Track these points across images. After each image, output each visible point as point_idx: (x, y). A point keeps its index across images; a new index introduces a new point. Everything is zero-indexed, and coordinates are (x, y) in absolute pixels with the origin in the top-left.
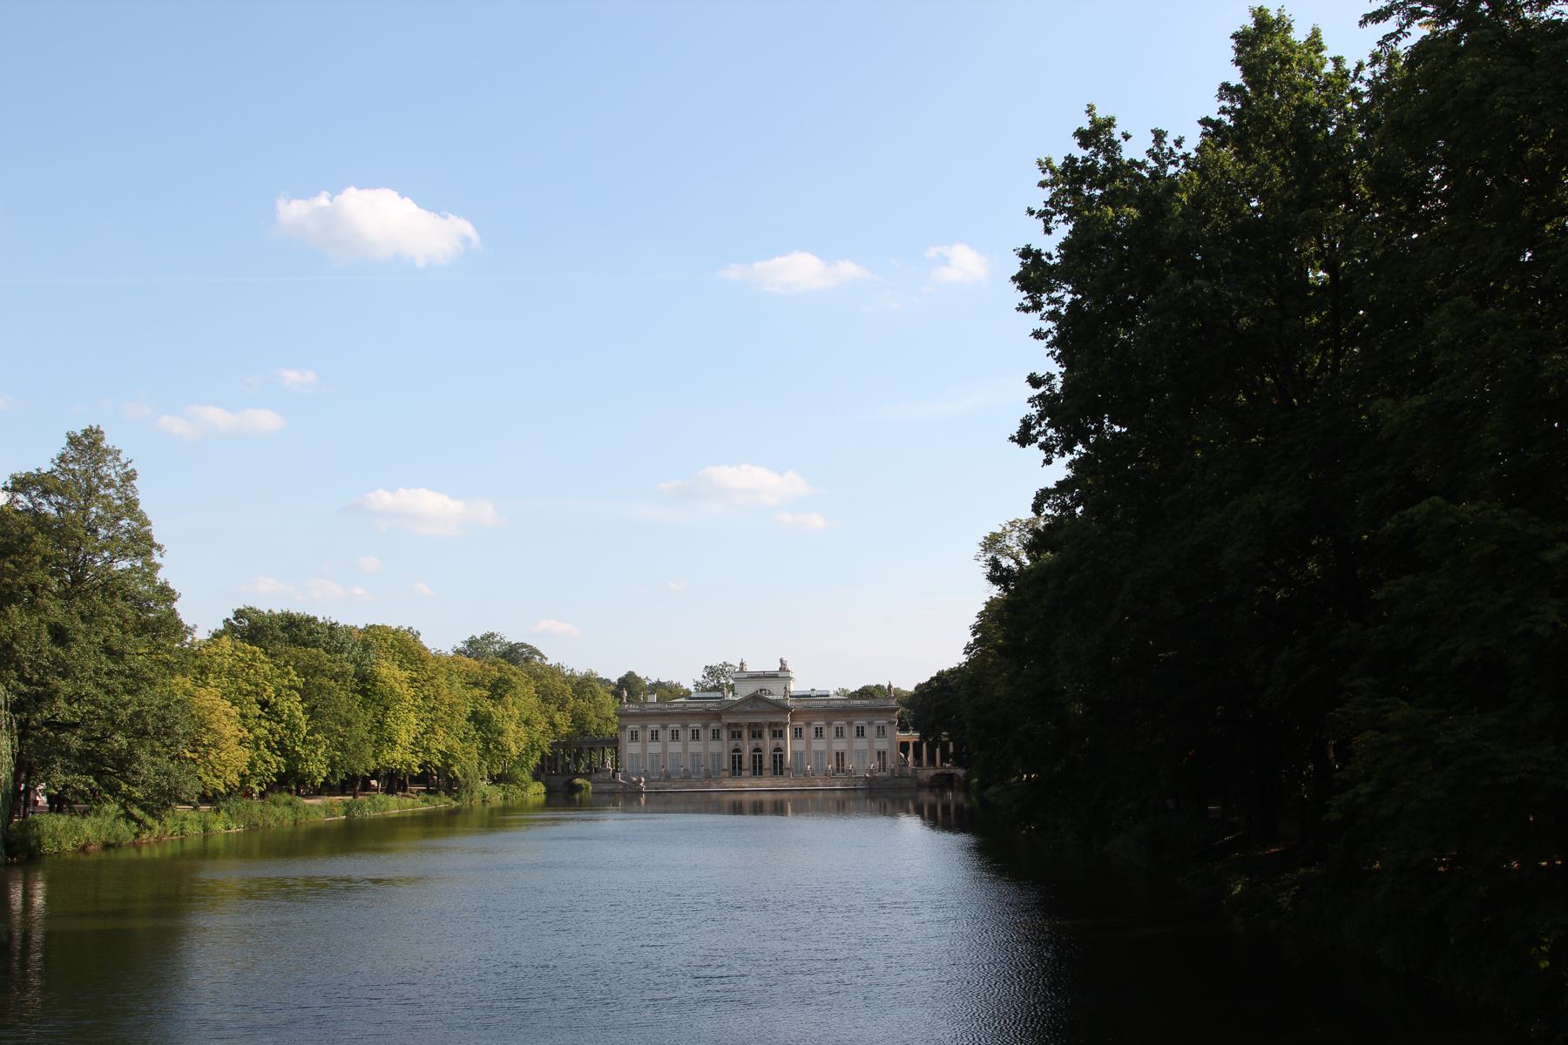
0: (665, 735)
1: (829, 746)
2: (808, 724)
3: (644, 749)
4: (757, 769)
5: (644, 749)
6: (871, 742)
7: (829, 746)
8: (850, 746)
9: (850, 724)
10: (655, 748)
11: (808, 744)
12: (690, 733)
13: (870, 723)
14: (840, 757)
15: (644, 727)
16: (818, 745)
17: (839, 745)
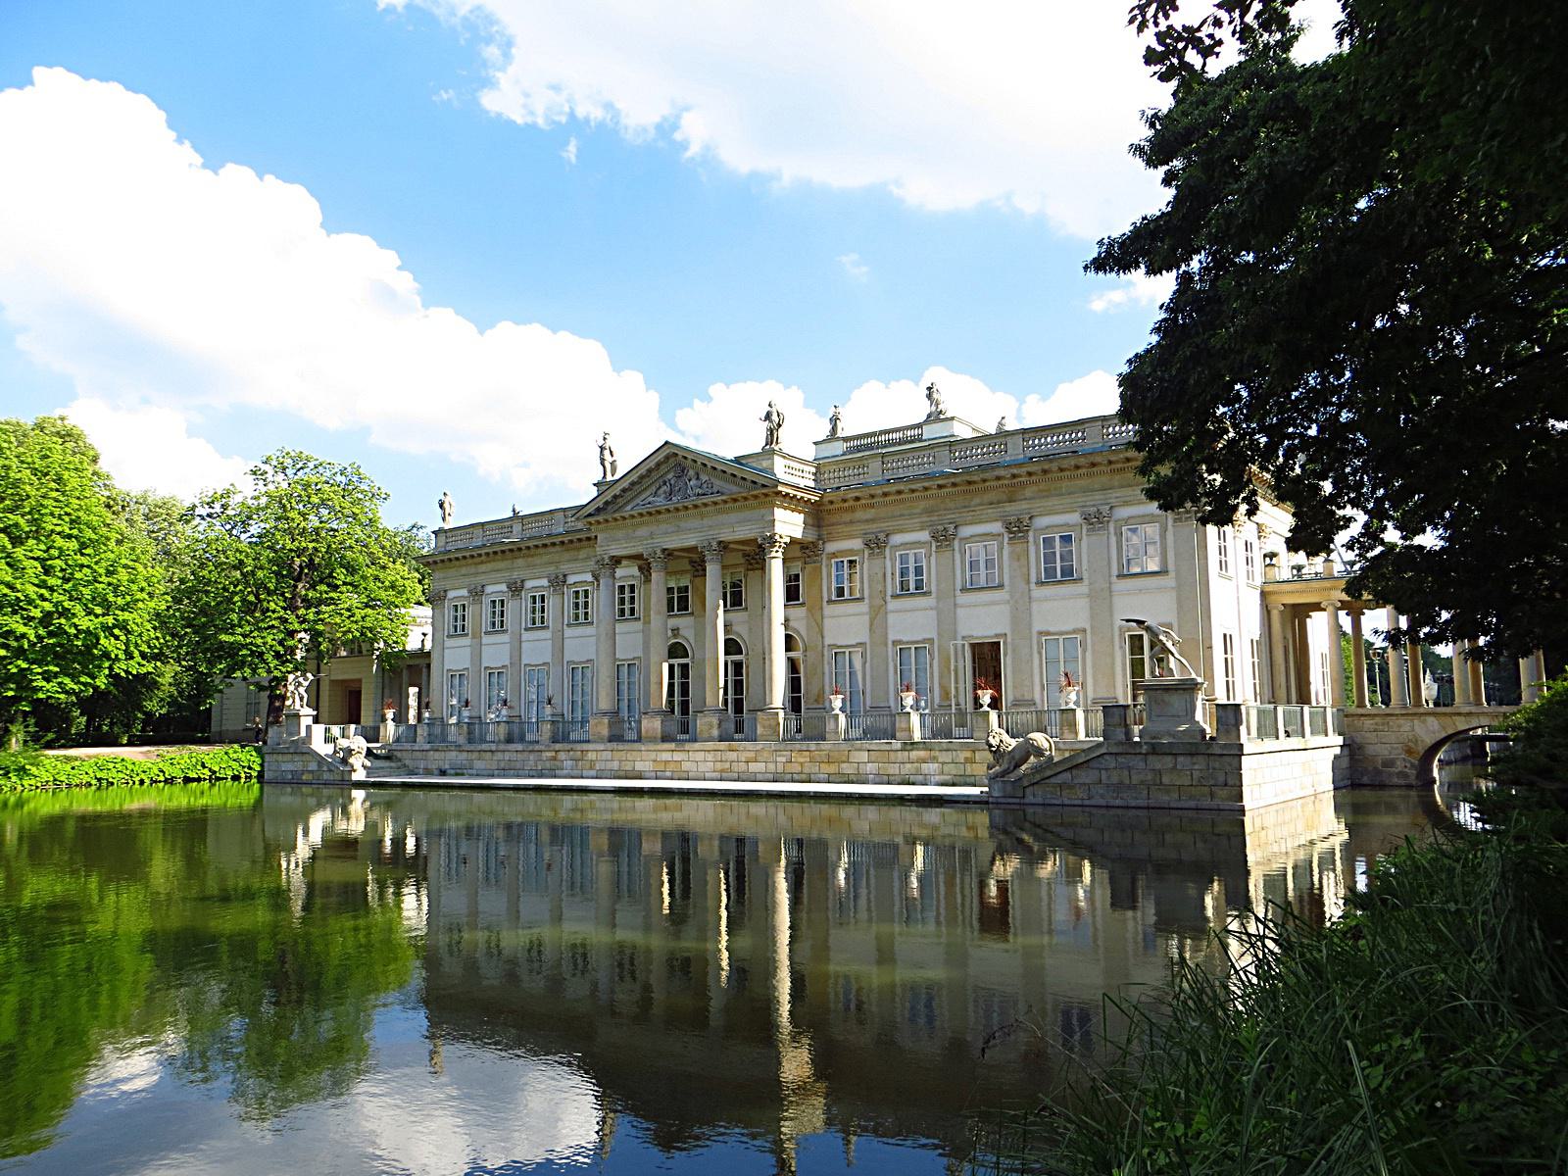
0: (517, 611)
1: (947, 621)
2: (876, 545)
3: (477, 655)
4: (740, 714)
5: (477, 655)
6: (1101, 601)
7: (947, 621)
8: (1021, 616)
9: (1017, 529)
10: (496, 652)
11: (878, 618)
12: (569, 600)
13: (1095, 520)
14: (987, 661)
15: (477, 593)
16: (911, 621)
17: (982, 619)
